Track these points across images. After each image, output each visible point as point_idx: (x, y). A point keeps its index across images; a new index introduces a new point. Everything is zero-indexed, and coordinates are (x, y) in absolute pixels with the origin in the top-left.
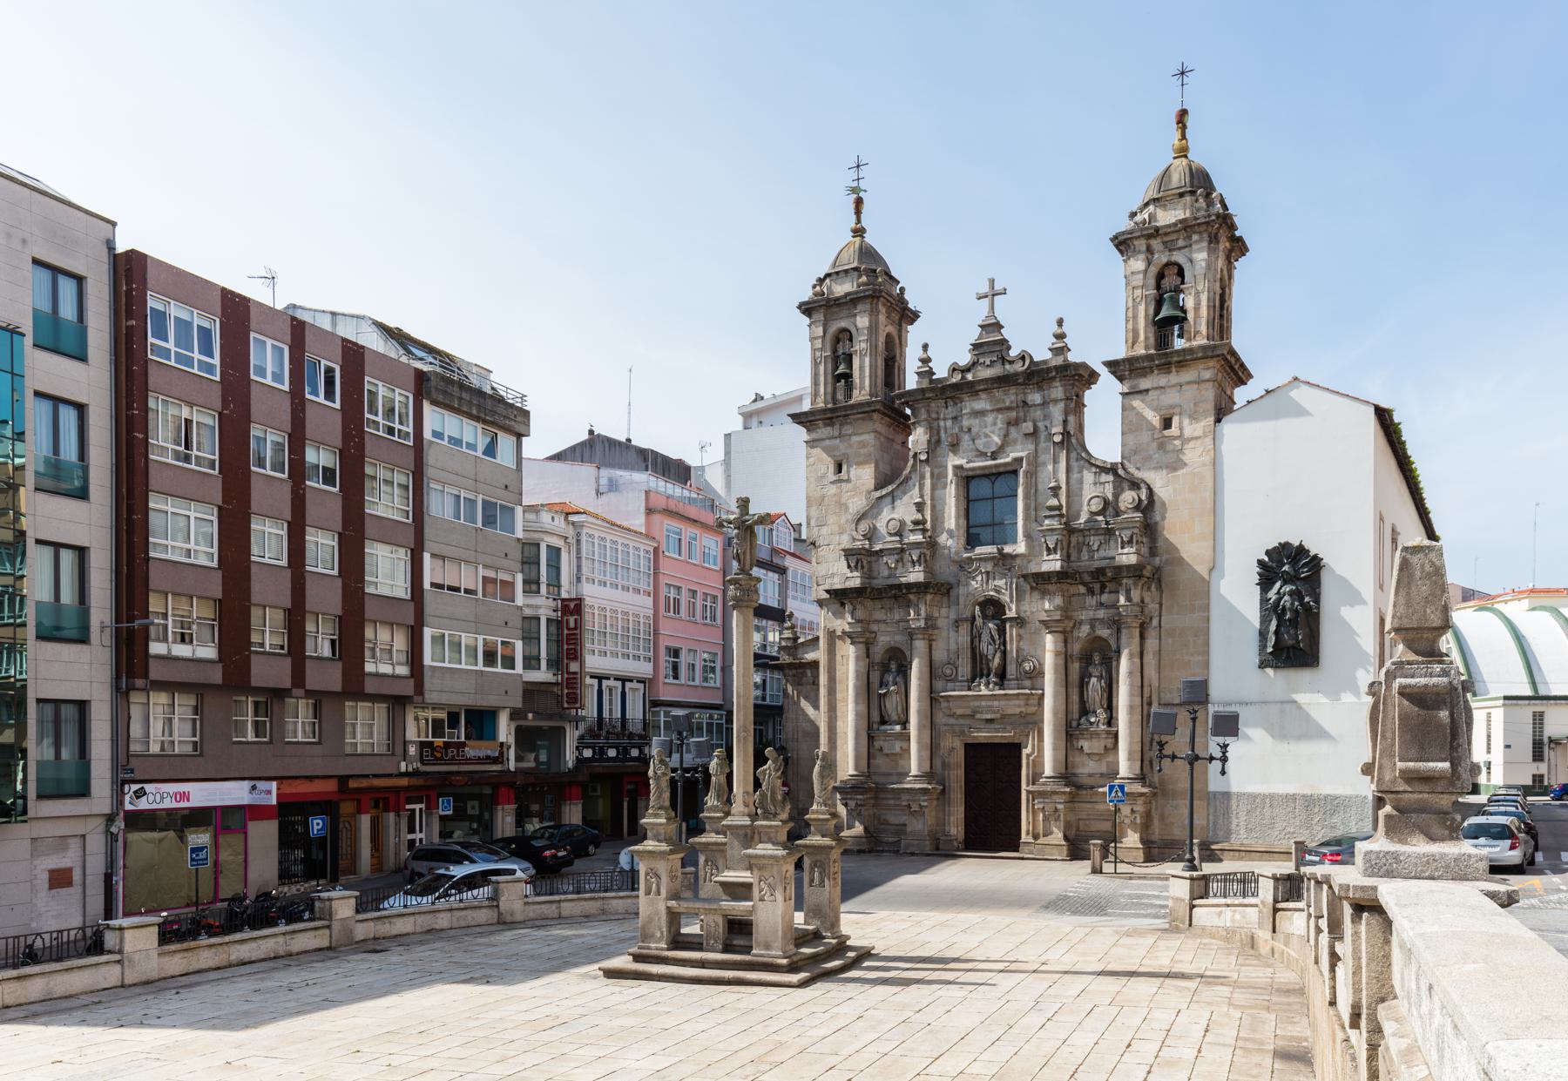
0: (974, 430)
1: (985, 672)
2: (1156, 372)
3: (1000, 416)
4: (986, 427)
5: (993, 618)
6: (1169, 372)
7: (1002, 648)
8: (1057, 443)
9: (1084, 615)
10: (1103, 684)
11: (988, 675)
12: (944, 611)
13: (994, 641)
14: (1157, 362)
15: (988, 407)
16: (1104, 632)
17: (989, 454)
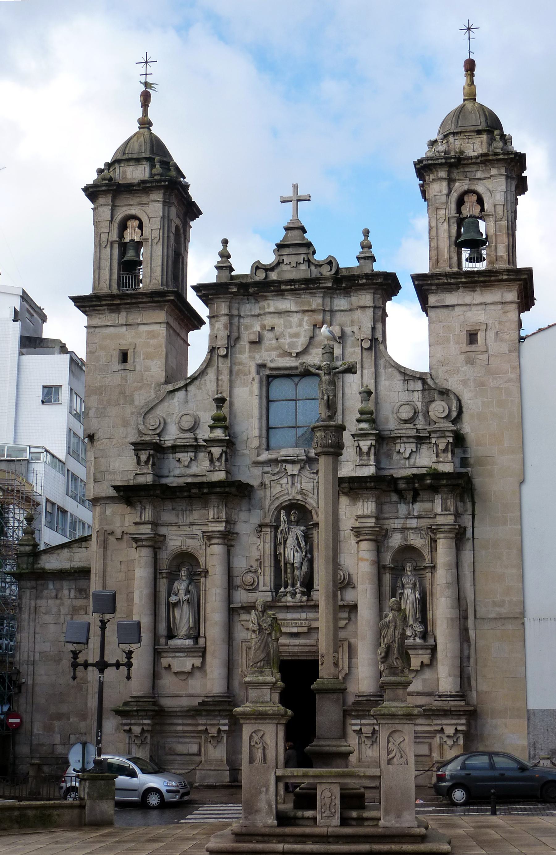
0: (278, 330)
1: (290, 582)
2: (461, 289)
3: (306, 318)
4: (291, 327)
5: (297, 523)
6: (474, 291)
7: (309, 556)
8: (366, 349)
9: (397, 524)
10: (418, 596)
11: (293, 585)
12: (243, 515)
13: (300, 547)
14: (463, 280)
15: (293, 308)
16: (417, 541)
17: (294, 355)
